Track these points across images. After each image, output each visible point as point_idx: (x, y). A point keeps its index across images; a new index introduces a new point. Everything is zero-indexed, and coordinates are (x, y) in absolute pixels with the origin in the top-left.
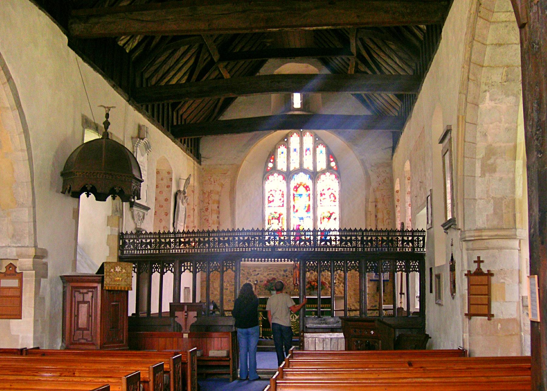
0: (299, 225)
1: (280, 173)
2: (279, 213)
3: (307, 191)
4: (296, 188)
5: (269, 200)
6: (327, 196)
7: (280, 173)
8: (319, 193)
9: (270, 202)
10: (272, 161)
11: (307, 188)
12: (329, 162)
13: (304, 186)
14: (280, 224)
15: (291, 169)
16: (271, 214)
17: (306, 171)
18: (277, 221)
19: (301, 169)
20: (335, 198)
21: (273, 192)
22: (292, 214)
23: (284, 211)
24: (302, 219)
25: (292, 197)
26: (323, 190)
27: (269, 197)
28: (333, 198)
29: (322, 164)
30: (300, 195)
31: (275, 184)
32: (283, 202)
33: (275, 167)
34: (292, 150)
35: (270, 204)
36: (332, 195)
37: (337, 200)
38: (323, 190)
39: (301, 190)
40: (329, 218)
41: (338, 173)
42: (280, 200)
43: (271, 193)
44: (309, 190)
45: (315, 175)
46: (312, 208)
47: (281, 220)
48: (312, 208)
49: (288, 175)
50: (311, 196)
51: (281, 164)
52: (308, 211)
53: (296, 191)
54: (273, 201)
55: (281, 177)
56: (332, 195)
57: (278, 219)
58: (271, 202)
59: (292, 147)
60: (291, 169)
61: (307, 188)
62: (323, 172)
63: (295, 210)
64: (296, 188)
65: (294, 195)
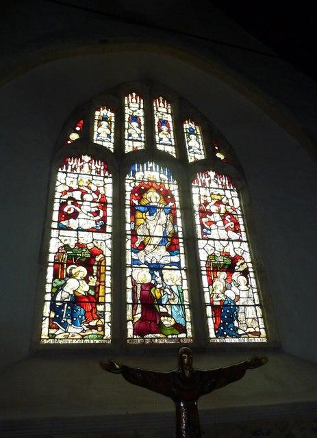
0: (150, 286)
1: (98, 153)
2: (90, 246)
3: (167, 202)
4: (140, 192)
5: (61, 211)
6: (217, 217)
7: (98, 153)
8: (196, 208)
9: (65, 216)
10: (78, 129)
11: (166, 195)
12: (209, 149)
13: (158, 191)
14: (93, 281)
15: (128, 149)
16: (66, 247)
17: (161, 159)
18: (83, 271)
19: (150, 153)
20: (237, 224)
21: (77, 195)
22: (129, 256)
23: (104, 242)
24: (155, 268)
25: (128, 211)
26: (206, 203)
27: (63, 205)
28: (230, 224)
29: (196, 149)
30: (151, 209)
31: (81, 180)
32: (104, 219)
33: (87, 134)
34: (127, 117)
35: (64, 223)
36: (228, 217)
37: (242, 228)
38: (206, 203)
39: (153, 197)
40: (230, 269)
41: (235, 173)
42: (97, 213)
43: (69, 194)
44: (173, 200)
45: (183, 170)
46: (185, 241)
47: (95, 268)
48: (185, 241)
49: (118, 163)
50: (179, 213)
51: (103, 134)
52: (172, 249)
53: (140, 198)
54: (75, 215)
55: (99, 166)
56: (229, 217)
57: (88, 264)
58: (69, 217)
59: (127, 110)
60: (128, 149)
61: (166, 195)
62: (203, 166)
63: (137, 244)
64: (140, 192)
65: (133, 206)
